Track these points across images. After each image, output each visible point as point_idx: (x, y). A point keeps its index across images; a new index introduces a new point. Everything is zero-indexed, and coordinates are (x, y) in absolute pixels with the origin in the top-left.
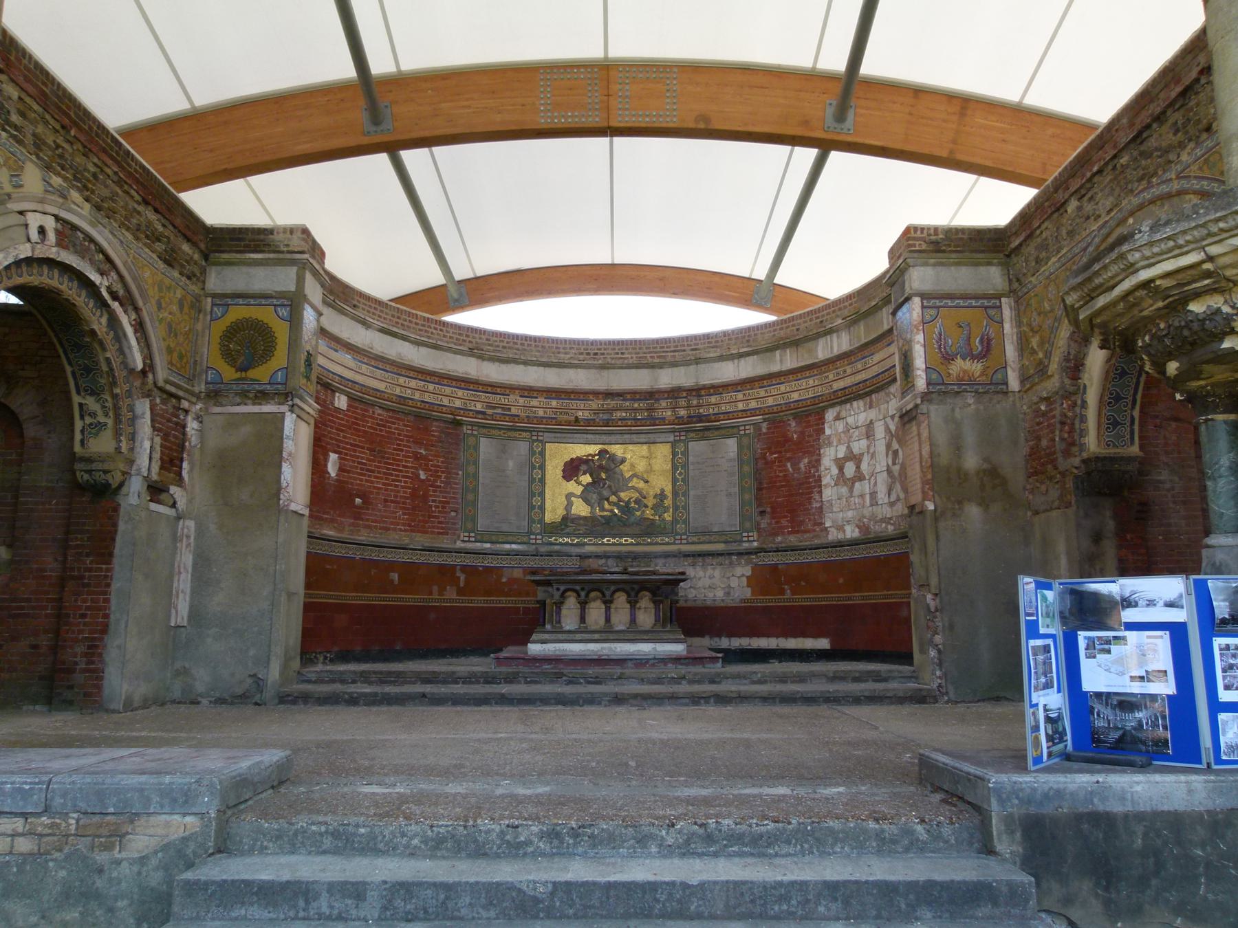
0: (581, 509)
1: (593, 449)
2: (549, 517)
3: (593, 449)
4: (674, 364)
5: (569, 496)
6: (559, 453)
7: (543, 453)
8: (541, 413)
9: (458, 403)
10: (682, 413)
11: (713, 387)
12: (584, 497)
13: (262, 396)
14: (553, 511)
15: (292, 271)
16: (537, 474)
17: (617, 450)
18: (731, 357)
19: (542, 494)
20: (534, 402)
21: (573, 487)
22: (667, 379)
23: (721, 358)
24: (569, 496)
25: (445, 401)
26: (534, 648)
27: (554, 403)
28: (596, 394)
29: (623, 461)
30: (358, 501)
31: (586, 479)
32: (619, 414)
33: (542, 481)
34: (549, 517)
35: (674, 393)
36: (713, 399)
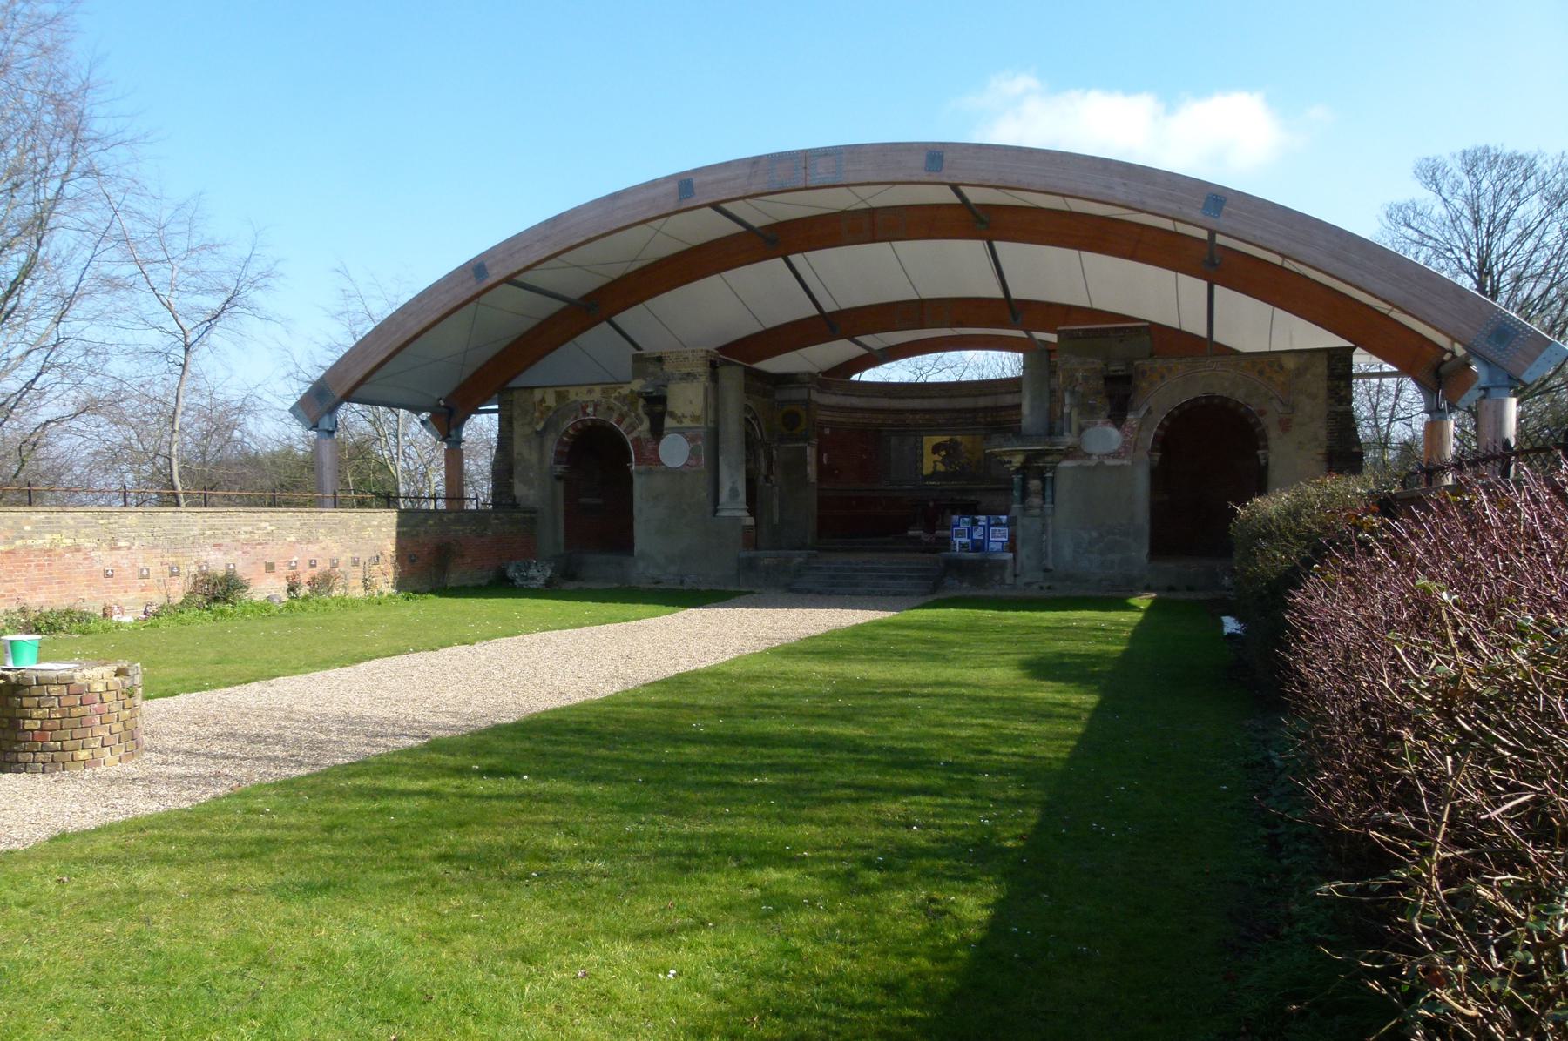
0: (941, 468)
1: (946, 438)
2: (925, 473)
3: (946, 438)
4: (985, 395)
5: (935, 462)
6: (930, 441)
7: (922, 442)
8: (920, 422)
9: (880, 421)
10: (989, 419)
11: (1002, 407)
12: (943, 462)
13: (797, 440)
14: (928, 468)
15: (806, 391)
16: (919, 452)
17: (959, 438)
18: (1010, 393)
19: (922, 462)
20: (918, 417)
21: (937, 457)
22: (983, 402)
23: (1007, 393)
24: (935, 462)
25: (874, 421)
26: (910, 533)
27: (927, 416)
28: (948, 410)
29: (961, 444)
30: (836, 472)
31: (943, 453)
32: (960, 420)
33: (922, 455)
34: (925, 473)
35: (985, 409)
36: (1003, 413)
